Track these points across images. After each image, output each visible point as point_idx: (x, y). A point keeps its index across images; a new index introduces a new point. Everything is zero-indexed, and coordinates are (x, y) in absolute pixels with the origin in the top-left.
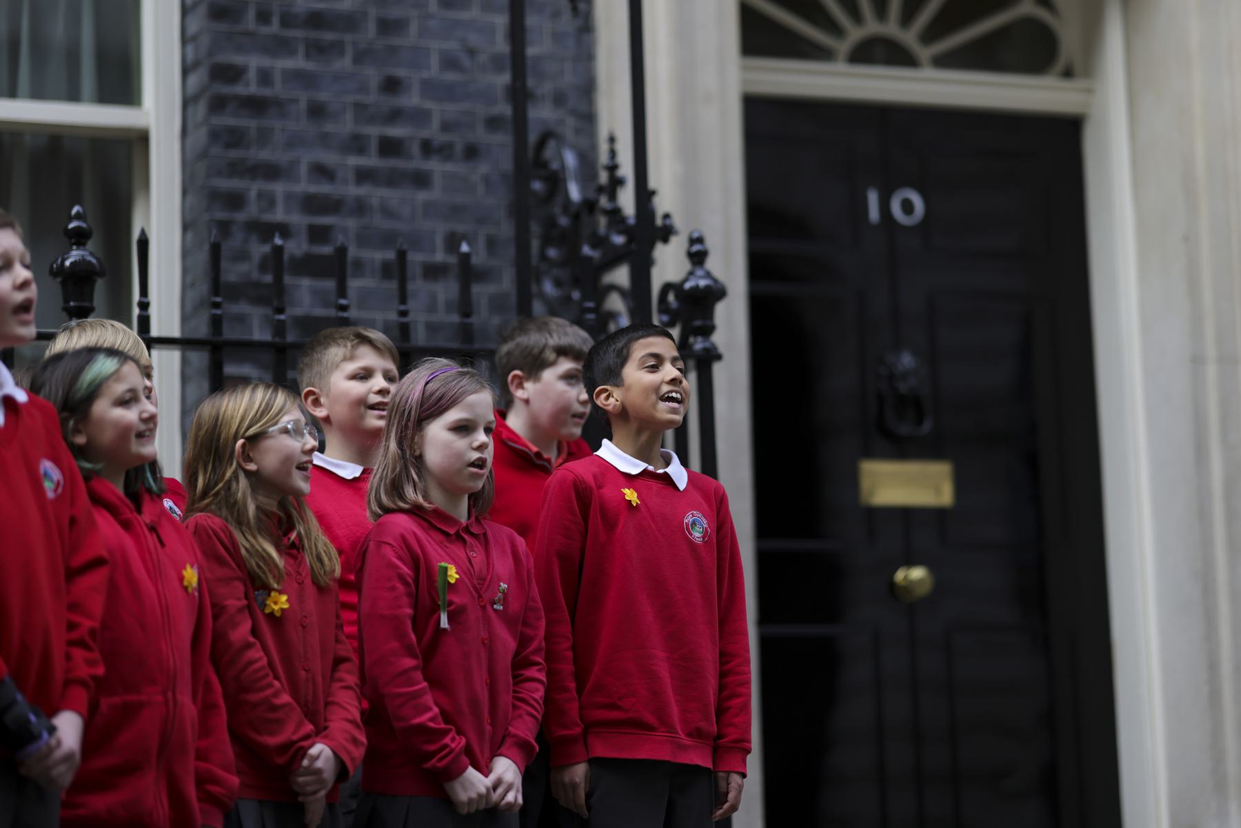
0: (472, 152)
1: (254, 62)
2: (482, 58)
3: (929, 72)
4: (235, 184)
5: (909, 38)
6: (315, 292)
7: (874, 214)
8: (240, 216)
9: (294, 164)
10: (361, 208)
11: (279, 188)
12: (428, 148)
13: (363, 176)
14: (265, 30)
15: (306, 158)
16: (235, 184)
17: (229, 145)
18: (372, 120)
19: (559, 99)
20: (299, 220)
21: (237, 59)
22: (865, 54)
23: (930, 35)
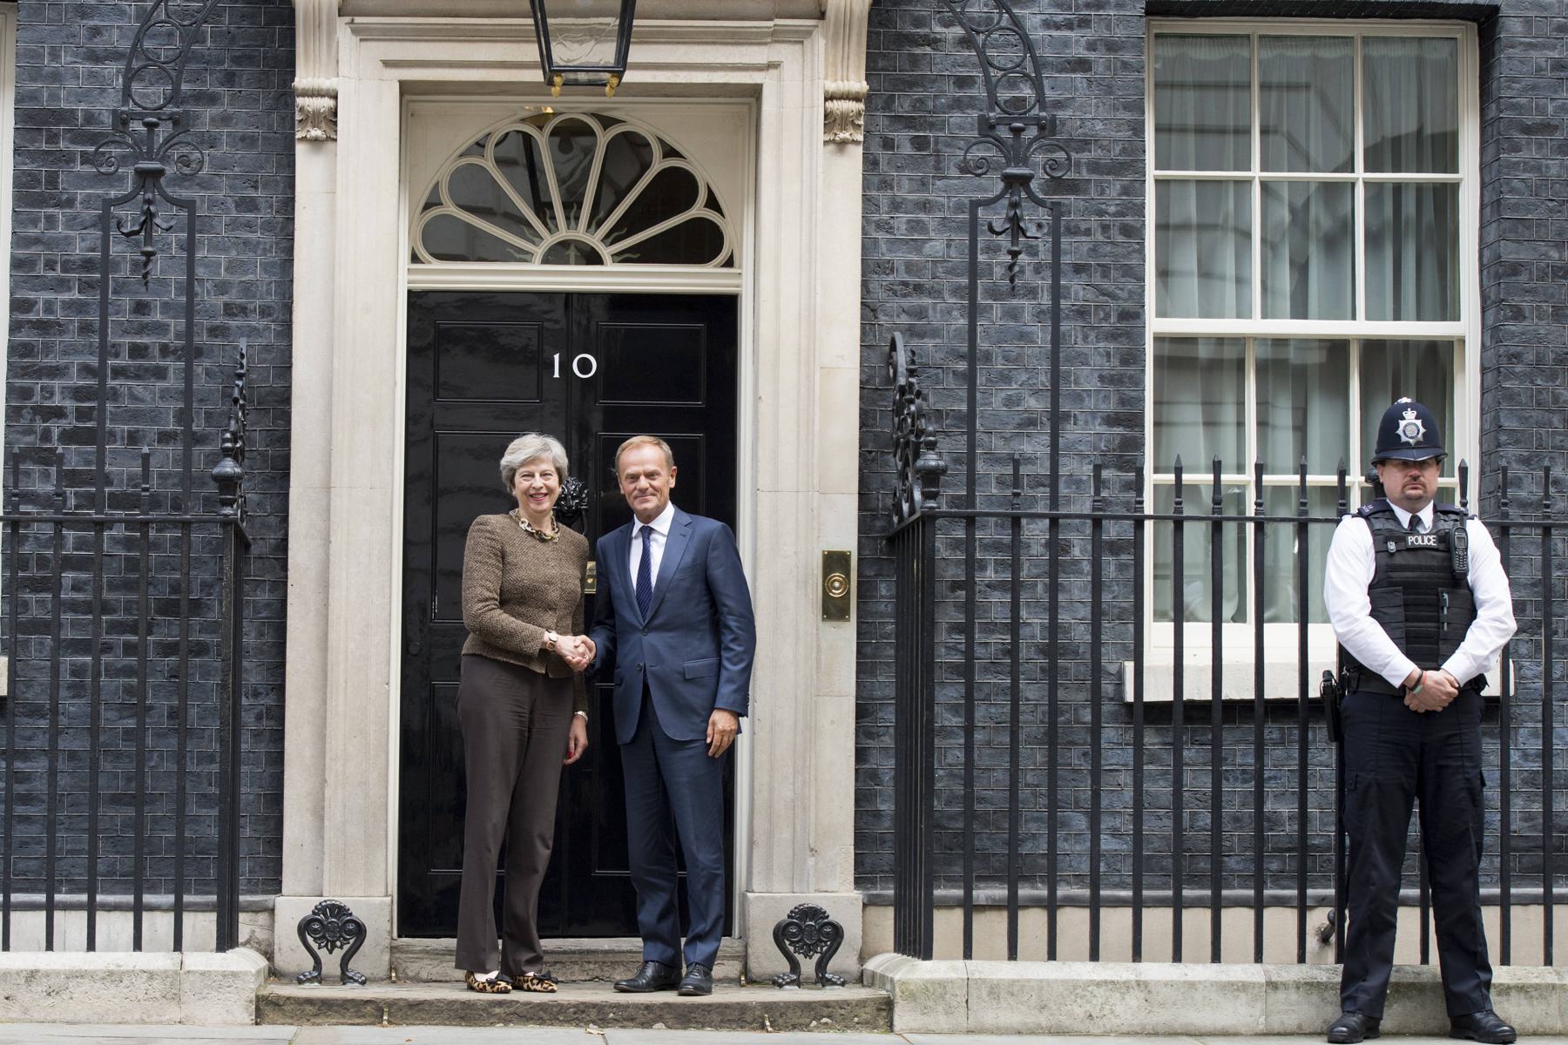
0: (199, 352)
1: (43, 296)
2: (208, 285)
3: (610, 266)
4: (26, 382)
5: (595, 240)
6: (79, 453)
7: (557, 375)
8: (29, 404)
9: (66, 367)
10: (115, 396)
11: (57, 383)
12: (165, 350)
13: (118, 372)
14: (51, 274)
15: (77, 360)
16: (26, 382)
17: (22, 356)
18: (126, 332)
19: (265, 312)
20: (69, 404)
21: (32, 295)
22: (557, 254)
23: (612, 237)
